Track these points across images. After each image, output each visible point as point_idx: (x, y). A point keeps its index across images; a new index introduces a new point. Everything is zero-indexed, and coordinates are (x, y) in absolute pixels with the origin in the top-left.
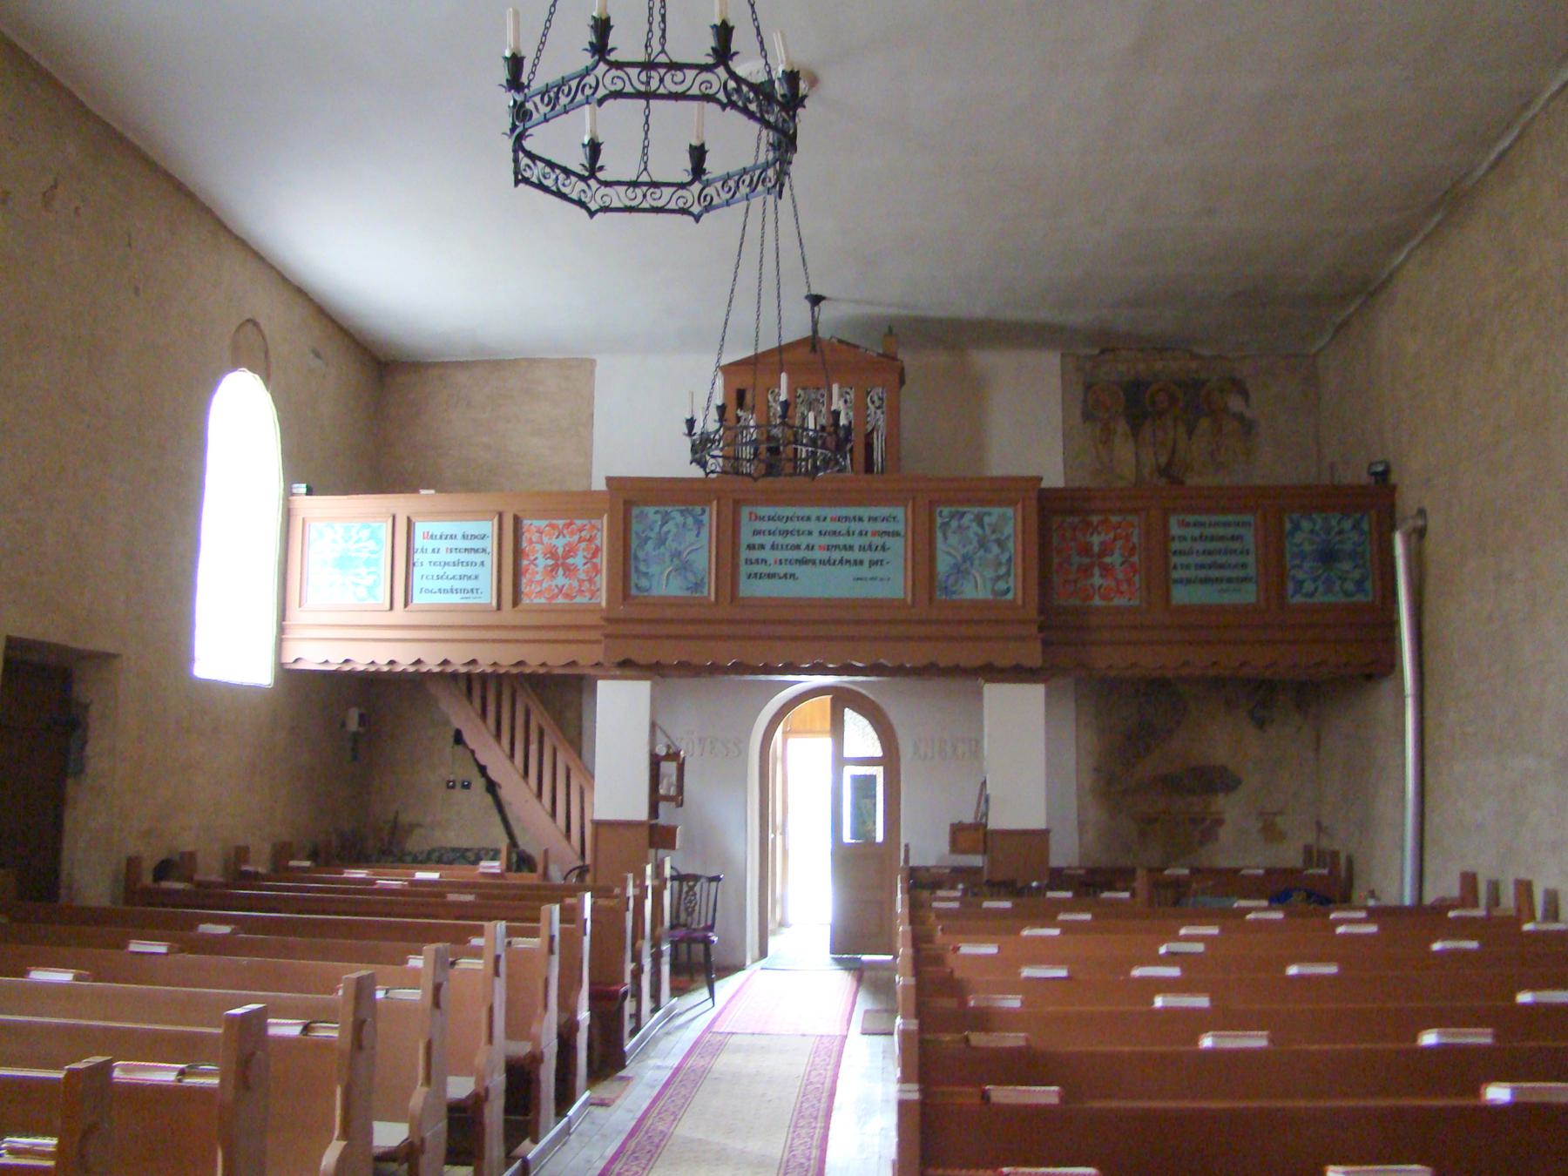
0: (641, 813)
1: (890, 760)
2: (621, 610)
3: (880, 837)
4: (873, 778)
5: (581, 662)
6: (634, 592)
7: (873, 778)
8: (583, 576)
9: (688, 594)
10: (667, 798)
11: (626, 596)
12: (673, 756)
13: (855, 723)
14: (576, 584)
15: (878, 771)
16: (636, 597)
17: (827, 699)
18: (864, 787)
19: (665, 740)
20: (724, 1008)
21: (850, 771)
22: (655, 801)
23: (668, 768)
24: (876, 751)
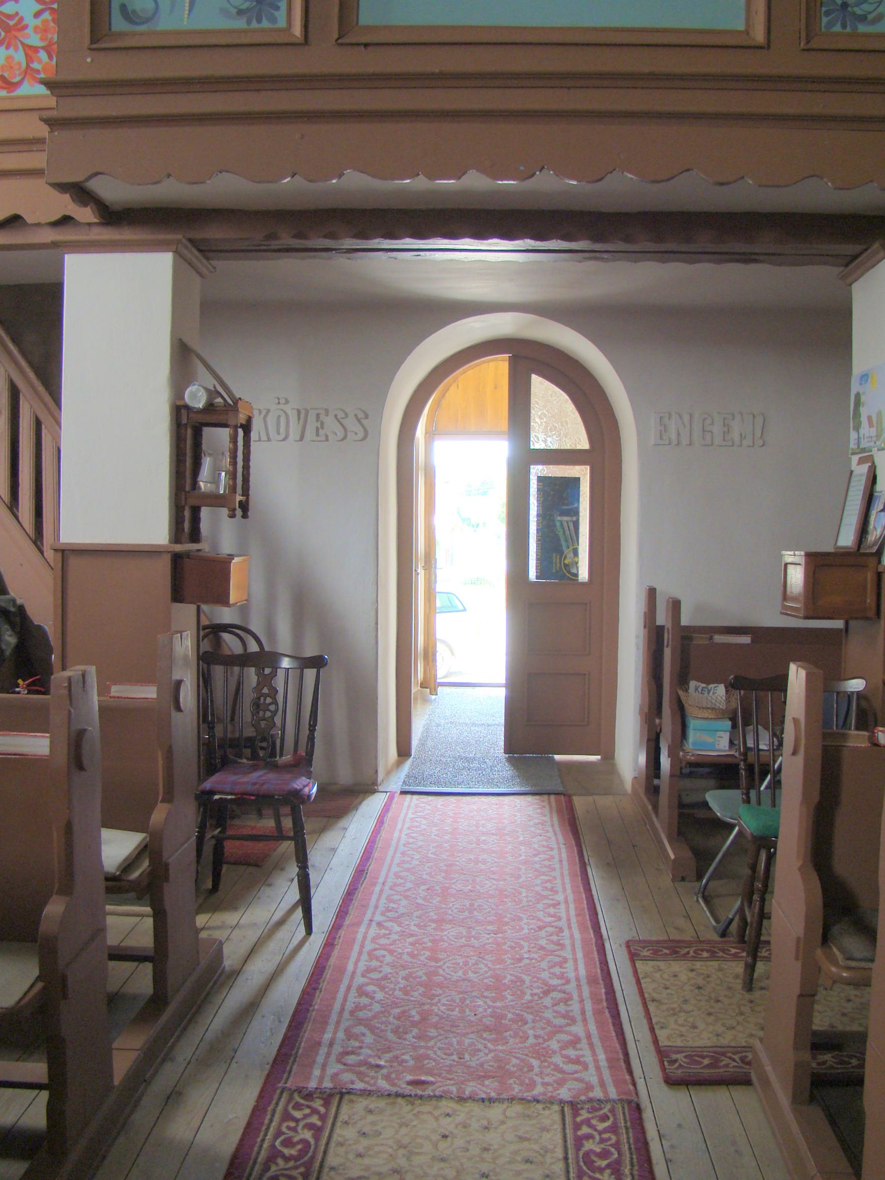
0: (153, 527)
1: (604, 450)
2: (91, 66)
3: (584, 574)
4: (575, 482)
5: (29, 220)
6: (118, 24)
7: (575, 482)
8: (34, 40)
9: (240, 24)
10: (216, 500)
11: (98, 32)
12: (222, 412)
13: (548, 398)
14: (20, 56)
15: (582, 473)
16: (122, 35)
17: (498, 367)
18: (559, 494)
19: (211, 383)
20: (337, 926)
21: (537, 471)
22: (187, 506)
23: (218, 438)
24: (578, 438)
